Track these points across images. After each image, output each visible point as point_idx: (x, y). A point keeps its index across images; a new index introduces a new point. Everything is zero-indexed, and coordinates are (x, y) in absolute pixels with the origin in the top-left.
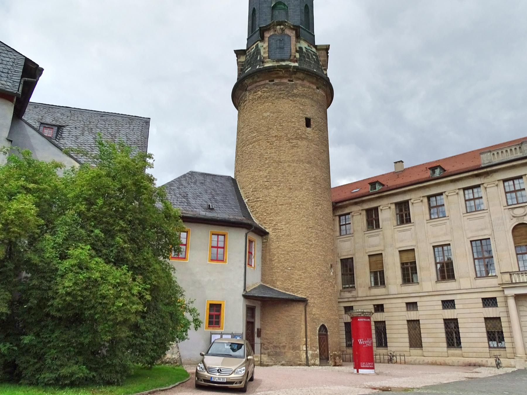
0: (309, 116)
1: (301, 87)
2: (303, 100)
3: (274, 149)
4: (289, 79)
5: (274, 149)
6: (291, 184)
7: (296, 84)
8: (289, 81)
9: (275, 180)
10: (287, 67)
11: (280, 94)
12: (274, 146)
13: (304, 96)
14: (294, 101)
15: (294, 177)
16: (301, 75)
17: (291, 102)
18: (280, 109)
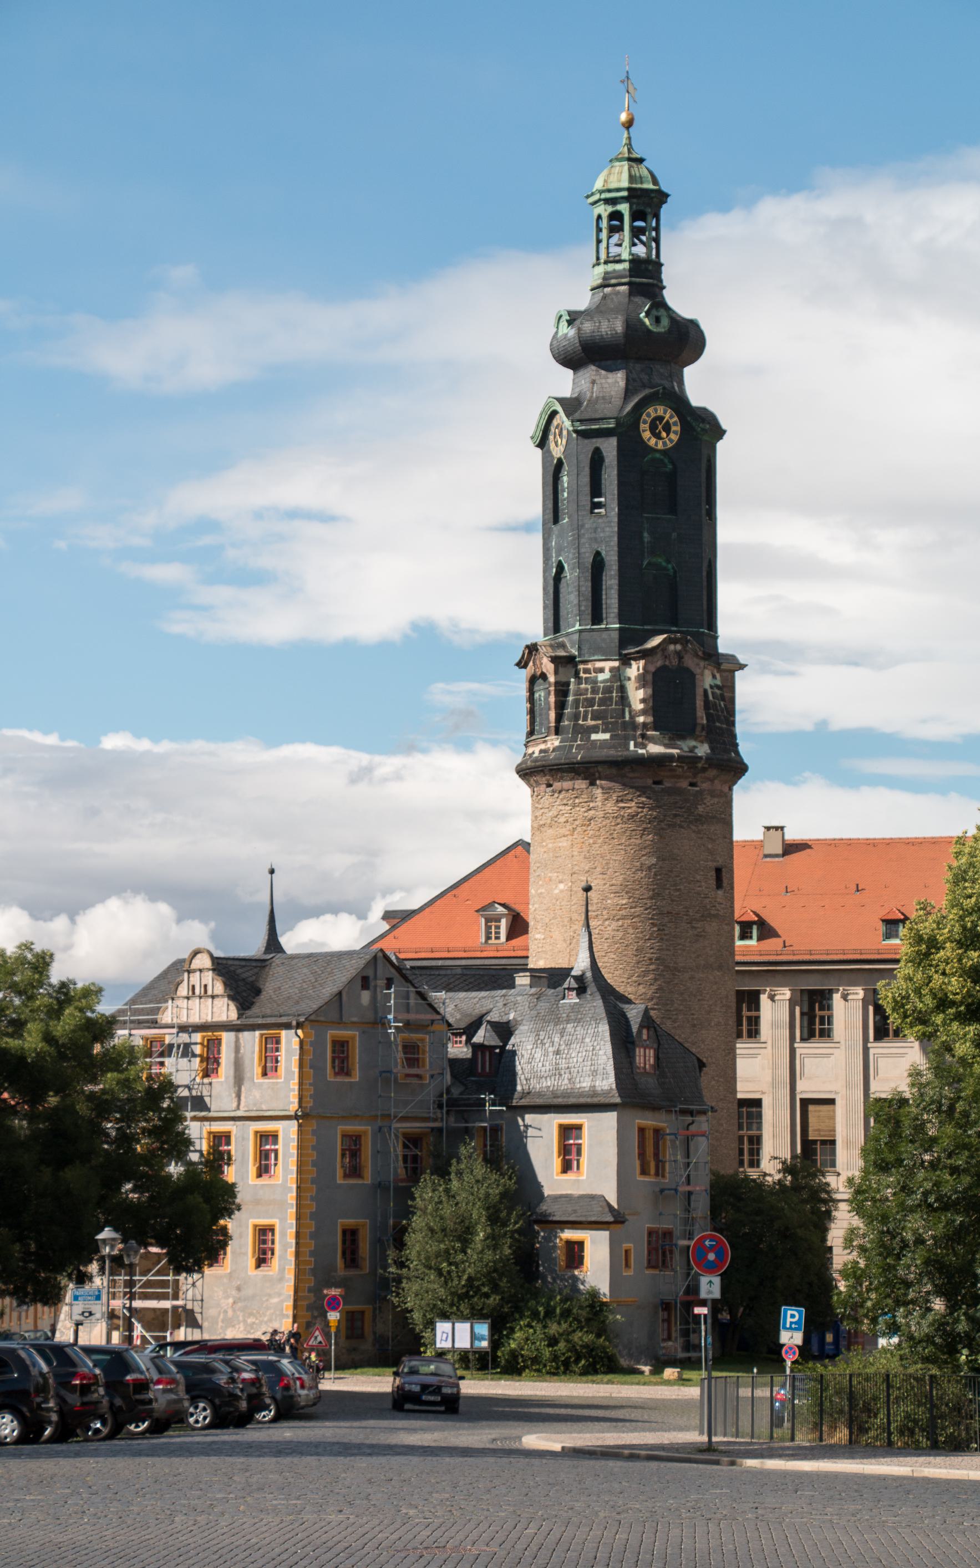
0: (720, 862)
1: (709, 797)
2: (713, 828)
3: (666, 940)
4: (690, 780)
5: (666, 940)
6: (695, 1017)
7: (701, 792)
8: (692, 784)
9: (668, 1007)
10: (690, 761)
11: (675, 815)
12: (665, 935)
13: (714, 817)
14: (699, 832)
15: (699, 1000)
16: (712, 773)
17: (693, 835)
18: (676, 851)
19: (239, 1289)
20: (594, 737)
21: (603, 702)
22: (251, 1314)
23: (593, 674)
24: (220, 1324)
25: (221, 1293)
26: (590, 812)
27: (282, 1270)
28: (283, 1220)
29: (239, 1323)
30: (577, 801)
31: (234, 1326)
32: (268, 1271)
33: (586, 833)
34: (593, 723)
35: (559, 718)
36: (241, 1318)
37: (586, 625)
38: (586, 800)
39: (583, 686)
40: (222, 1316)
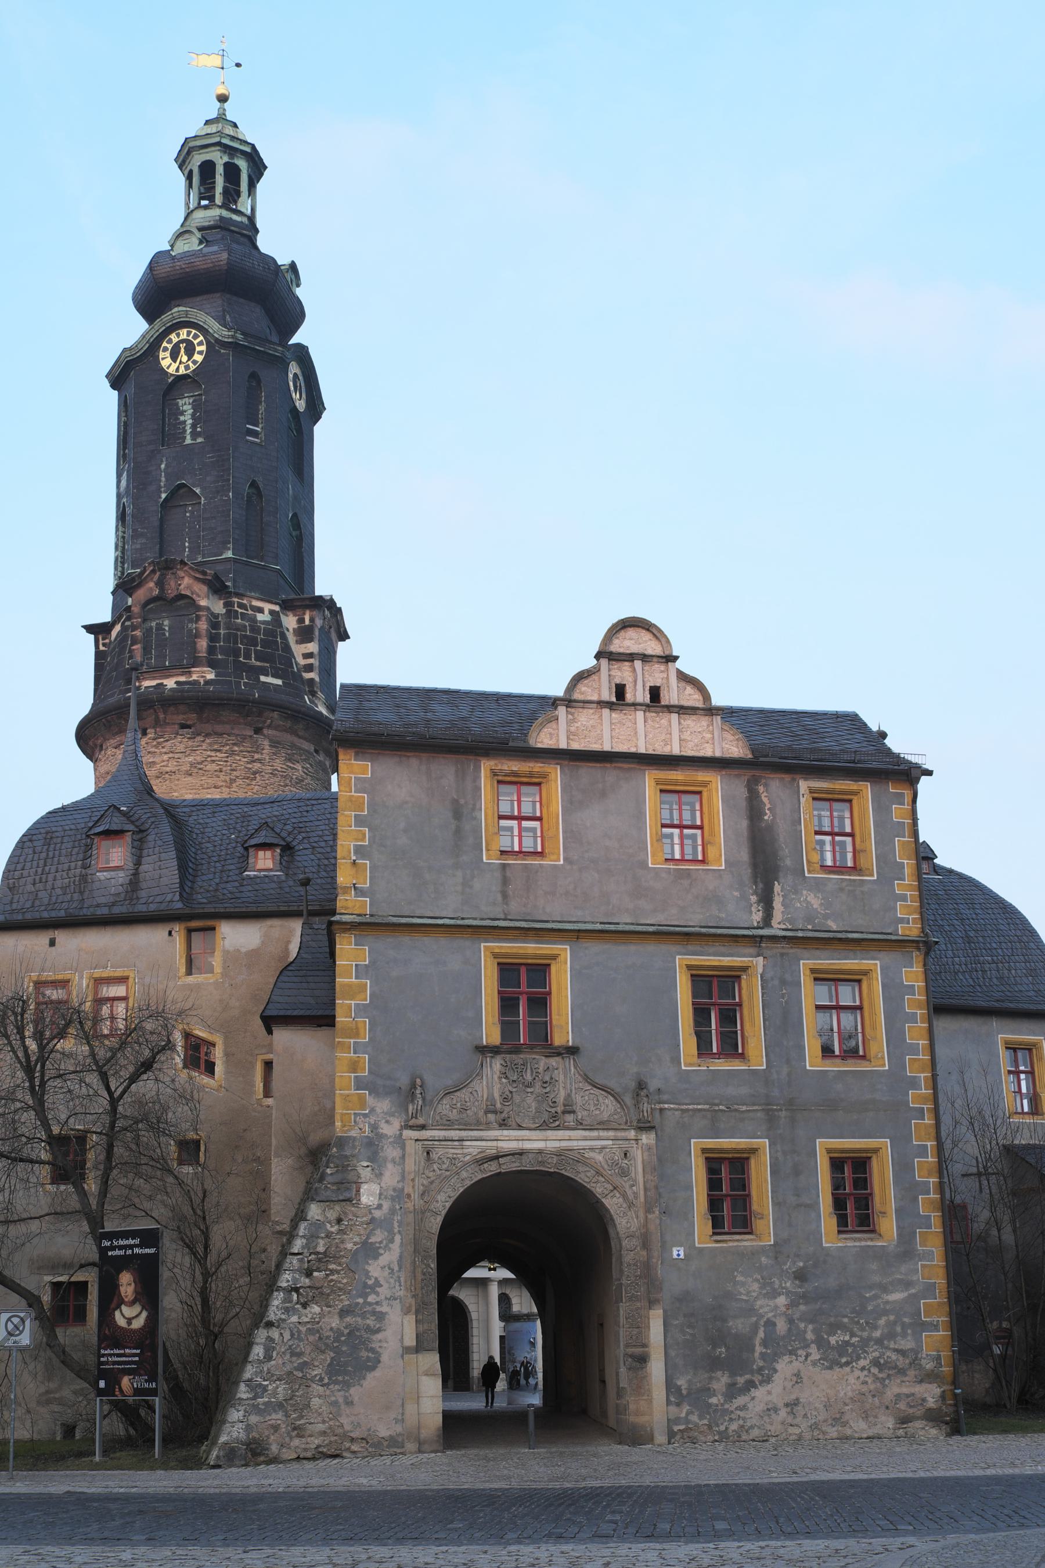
19: (800, 1276)
20: (263, 678)
21: (265, 644)
22: (833, 1328)
23: (250, 612)
24: (759, 1349)
25: (755, 1286)
26: (255, 764)
27: (906, 1237)
28: (901, 1140)
29: (808, 1346)
30: (236, 748)
31: (792, 1353)
32: (872, 1240)
33: (250, 787)
34: (258, 663)
35: (211, 650)
36: (810, 1336)
37: (242, 556)
38: (249, 749)
39: (239, 621)
40: (761, 1334)
